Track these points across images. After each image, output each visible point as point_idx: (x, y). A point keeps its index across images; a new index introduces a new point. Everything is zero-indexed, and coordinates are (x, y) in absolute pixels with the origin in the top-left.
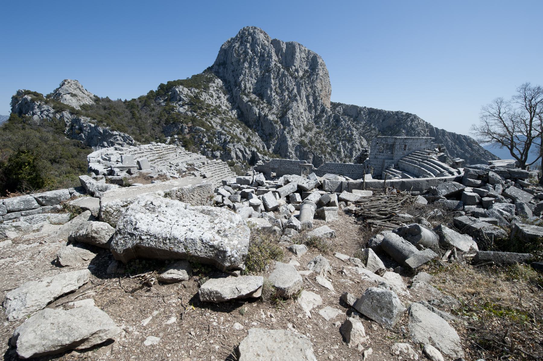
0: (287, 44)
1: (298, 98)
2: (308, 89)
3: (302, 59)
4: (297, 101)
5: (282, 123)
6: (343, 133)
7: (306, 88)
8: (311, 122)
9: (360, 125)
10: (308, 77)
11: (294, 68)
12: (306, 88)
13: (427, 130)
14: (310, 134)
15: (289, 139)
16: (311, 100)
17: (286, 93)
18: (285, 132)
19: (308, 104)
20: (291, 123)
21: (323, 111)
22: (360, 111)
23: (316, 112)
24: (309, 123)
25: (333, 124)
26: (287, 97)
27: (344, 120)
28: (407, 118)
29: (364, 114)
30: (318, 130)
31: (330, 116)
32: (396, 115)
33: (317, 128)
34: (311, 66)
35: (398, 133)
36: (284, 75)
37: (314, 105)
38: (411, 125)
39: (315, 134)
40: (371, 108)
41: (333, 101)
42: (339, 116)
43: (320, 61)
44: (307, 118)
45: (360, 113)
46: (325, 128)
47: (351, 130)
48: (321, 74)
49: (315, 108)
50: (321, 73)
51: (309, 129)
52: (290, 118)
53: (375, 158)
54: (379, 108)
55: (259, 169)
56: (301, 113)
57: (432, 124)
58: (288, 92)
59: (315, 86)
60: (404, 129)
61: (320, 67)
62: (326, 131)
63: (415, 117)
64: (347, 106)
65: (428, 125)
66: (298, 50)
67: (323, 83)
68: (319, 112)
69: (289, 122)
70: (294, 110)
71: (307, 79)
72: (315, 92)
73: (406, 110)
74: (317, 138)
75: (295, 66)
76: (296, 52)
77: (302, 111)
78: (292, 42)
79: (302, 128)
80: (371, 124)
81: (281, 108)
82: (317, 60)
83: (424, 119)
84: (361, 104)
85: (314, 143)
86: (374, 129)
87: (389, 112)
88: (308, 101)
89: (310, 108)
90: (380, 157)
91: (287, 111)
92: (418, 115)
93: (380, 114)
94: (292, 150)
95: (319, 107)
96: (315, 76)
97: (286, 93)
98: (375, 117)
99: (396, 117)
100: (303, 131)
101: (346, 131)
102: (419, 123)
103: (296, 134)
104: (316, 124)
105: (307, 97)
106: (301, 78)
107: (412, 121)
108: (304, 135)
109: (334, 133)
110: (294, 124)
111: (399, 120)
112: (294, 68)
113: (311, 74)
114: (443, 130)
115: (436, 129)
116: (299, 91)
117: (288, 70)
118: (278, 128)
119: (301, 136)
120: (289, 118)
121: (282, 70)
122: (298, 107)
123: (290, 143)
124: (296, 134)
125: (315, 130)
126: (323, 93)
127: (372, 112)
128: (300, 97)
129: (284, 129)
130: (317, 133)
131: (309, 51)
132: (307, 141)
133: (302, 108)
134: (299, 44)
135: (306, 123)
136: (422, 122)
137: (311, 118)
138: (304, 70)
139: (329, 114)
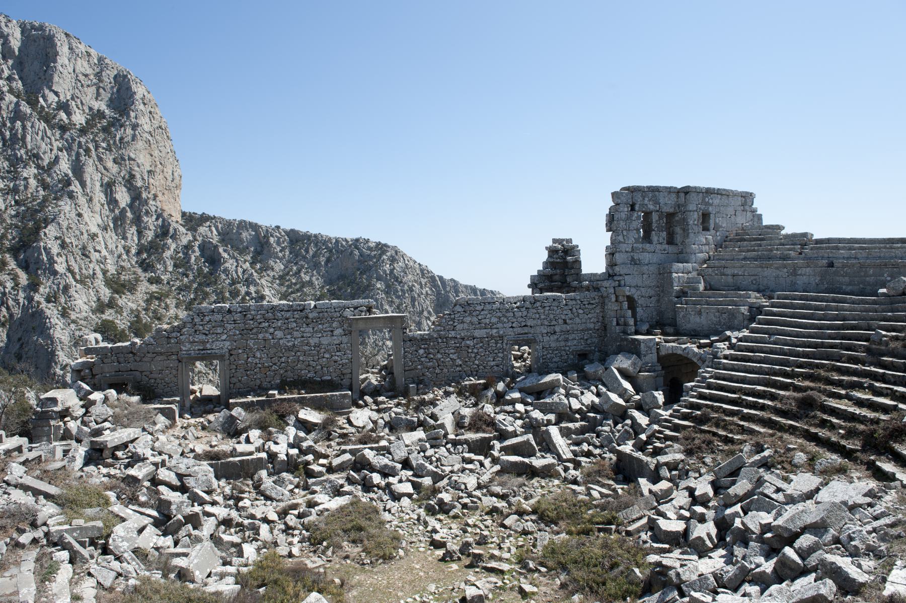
0: (23, 28)
1: (76, 187)
2: (110, 164)
3: (81, 77)
4: (71, 196)
5: (25, 266)
6: (235, 294)
7: (100, 159)
8: (127, 265)
9: (272, 274)
10: (105, 130)
11: (52, 98)
12: (100, 159)
13: (423, 281)
14: (128, 302)
15: (54, 321)
16: (123, 197)
17: (30, 172)
18: (37, 297)
19: (112, 211)
20: (60, 268)
21: (164, 231)
22: (266, 237)
23: (140, 233)
24: (122, 267)
25: (200, 270)
26: (33, 182)
27: (233, 257)
28: (381, 255)
29: (278, 243)
30: (154, 288)
31: (188, 247)
32: (357, 247)
33: (151, 281)
34: (111, 100)
35: (364, 290)
36: (17, 115)
37: (132, 209)
38: (392, 271)
39: (148, 301)
40: (292, 230)
41: (188, 209)
42: (216, 247)
43: (139, 91)
44: (112, 252)
45: (268, 242)
46: (178, 283)
47: (256, 284)
48: (147, 128)
49: (137, 220)
50: (145, 123)
51: (123, 286)
52: (55, 250)
53: (634, 262)
54: (313, 231)
55: (109, 369)
56: (93, 236)
57: (430, 268)
58: (38, 167)
59: (130, 159)
60: (379, 279)
61: (142, 107)
62: (180, 289)
63: (396, 252)
64: (229, 224)
65: (424, 272)
66: (63, 50)
67: (156, 153)
68: (150, 235)
69: (52, 261)
70: (65, 224)
71: (101, 135)
72: (132, 176)
73: (375, 237)
74: (155, 312)
75: (56, 94)
76: (57, 54)
77: (94, 229)
78: (41, 28)
79: (100, 282)
80: (299, 271)
81: (12, 217)
82: (129, 88)
83: (414, 258)
84: (265, 220)
85: (147, 328)
86: (310, 283)
87: (337, 241)
88: (112, 202)
89: (119, 222)
90: (646, 257)
91: (37, 230)
92: (402, 248)
93: (316, 245)
94: (71, 356)
95: (150, 221)
96: (129, 131)
97: (30, 172)
98: (307, 251)
99: (356, 252)
100: (106, 293)
101: (243, 289)
102: (406, 265)
103: (82, 301)
104: (145, 270)
105: (108, 188)
106: (83, 131)
107: (393, 260)
108: (111, 304)
109: (206, 295)
110: (69, 269)
111: (364, 258)
112: (52, 98)
113: (115, 123)
114: (452, 280)
115: (441, 278)
116: (78, 170)
117: (33, 103)
118: (9, 285)
119: (101, 307)
120: (48, 251)
121: (9, 98)
122: (80, 215)
123: (61, 332)
124: (82, 301)
125: (144, 287)
126: (156, 182)
127: (296, 239)
128: (83, 184)
129: (34, 286)
130: (151, 298)
131: (100, 59)
132: (122, 323)
133: (93, 221)
134: (67, 35)
135: (112, 269)
136: (411, 264)
137: (128, 252)
138: (91, 109)
139: (185, 241)
